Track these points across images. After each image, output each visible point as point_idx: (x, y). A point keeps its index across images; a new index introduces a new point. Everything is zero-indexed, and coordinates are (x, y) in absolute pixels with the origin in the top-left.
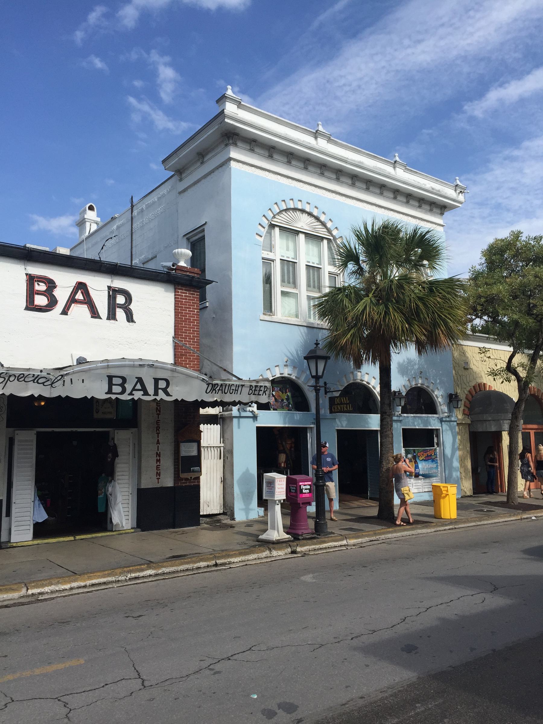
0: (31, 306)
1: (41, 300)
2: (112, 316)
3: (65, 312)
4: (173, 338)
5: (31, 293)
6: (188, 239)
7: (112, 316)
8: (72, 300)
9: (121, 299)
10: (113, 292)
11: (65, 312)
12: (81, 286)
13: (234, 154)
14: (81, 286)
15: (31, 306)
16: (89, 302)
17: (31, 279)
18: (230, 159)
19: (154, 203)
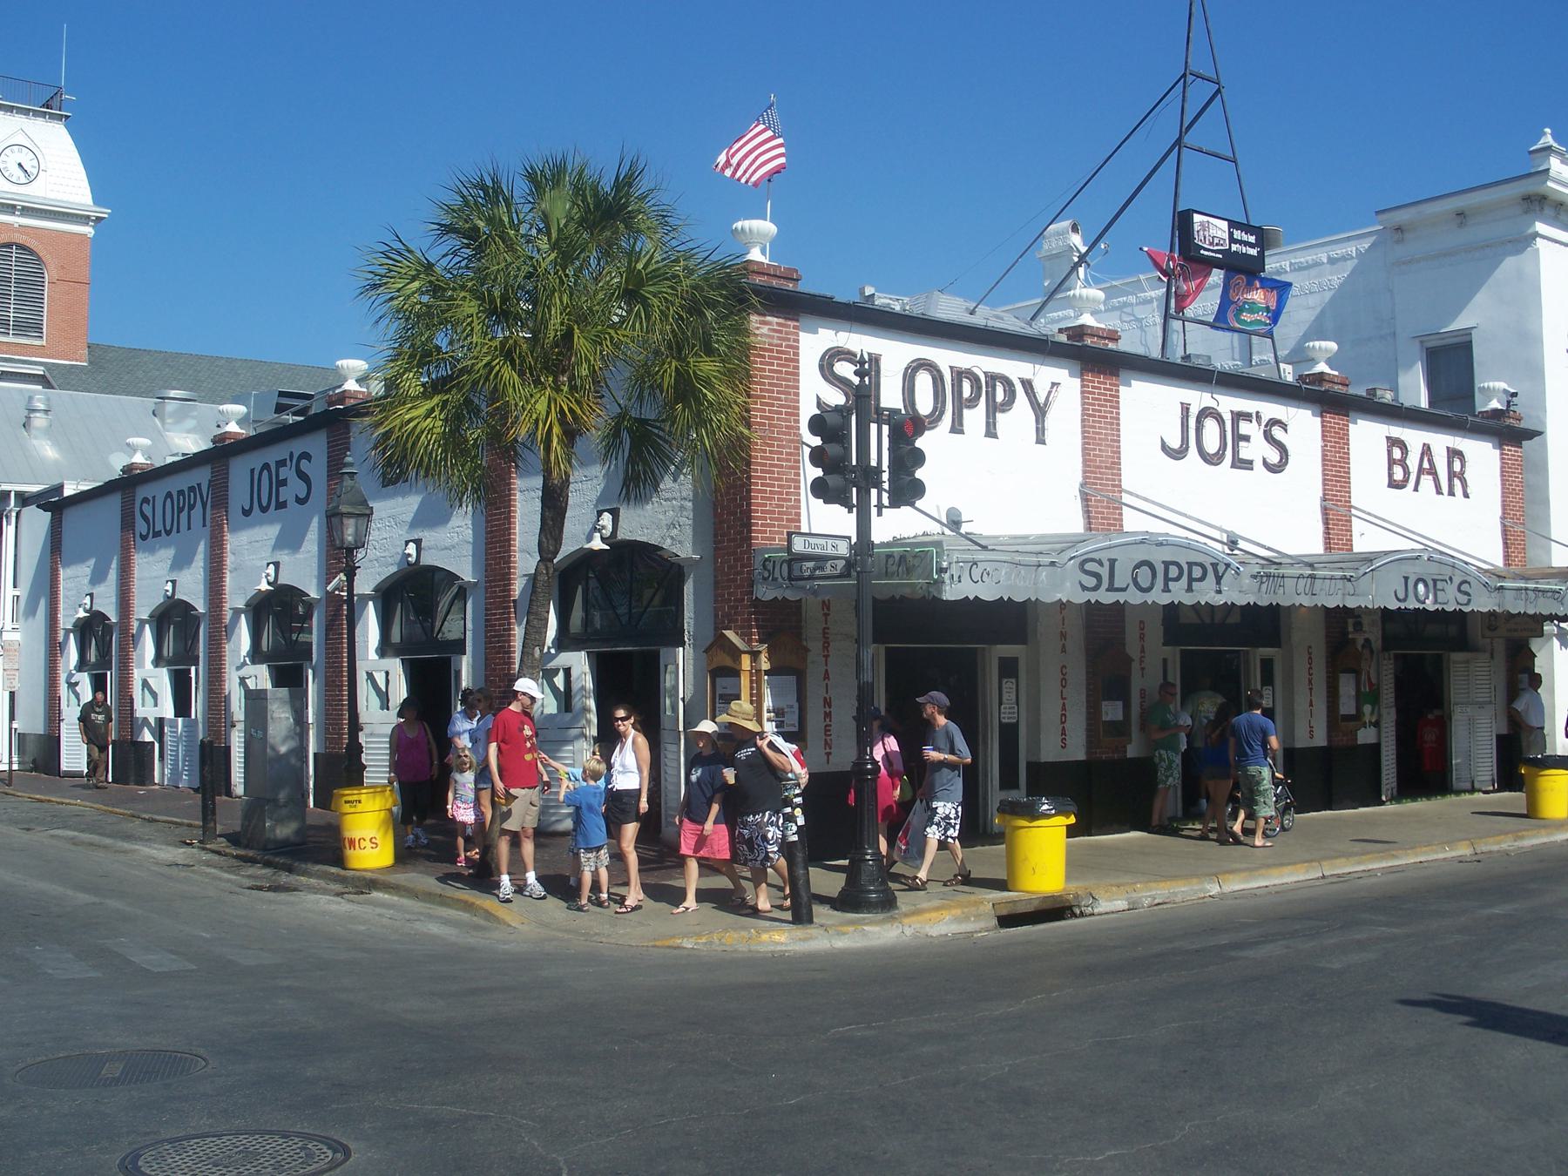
0: (1393, 484)
1: (1398, 474)
2: (1451, 493)
3: (1416, 489)
4: (1501, 518)
5: (1391, 462)
6: (1421, 342)
7: (1451, 493)
8: (1421, 471)
9: (1457, 466)
10: (1454, 454)
11: (1416, 489)
12: (1426, 450)
13: (1540, 227)
14: (1426, 450)
15: (1393, 484)
16: (1433, 472)
17: (1393, 442)
18: (1537, 235)
19: (1317, 264)
